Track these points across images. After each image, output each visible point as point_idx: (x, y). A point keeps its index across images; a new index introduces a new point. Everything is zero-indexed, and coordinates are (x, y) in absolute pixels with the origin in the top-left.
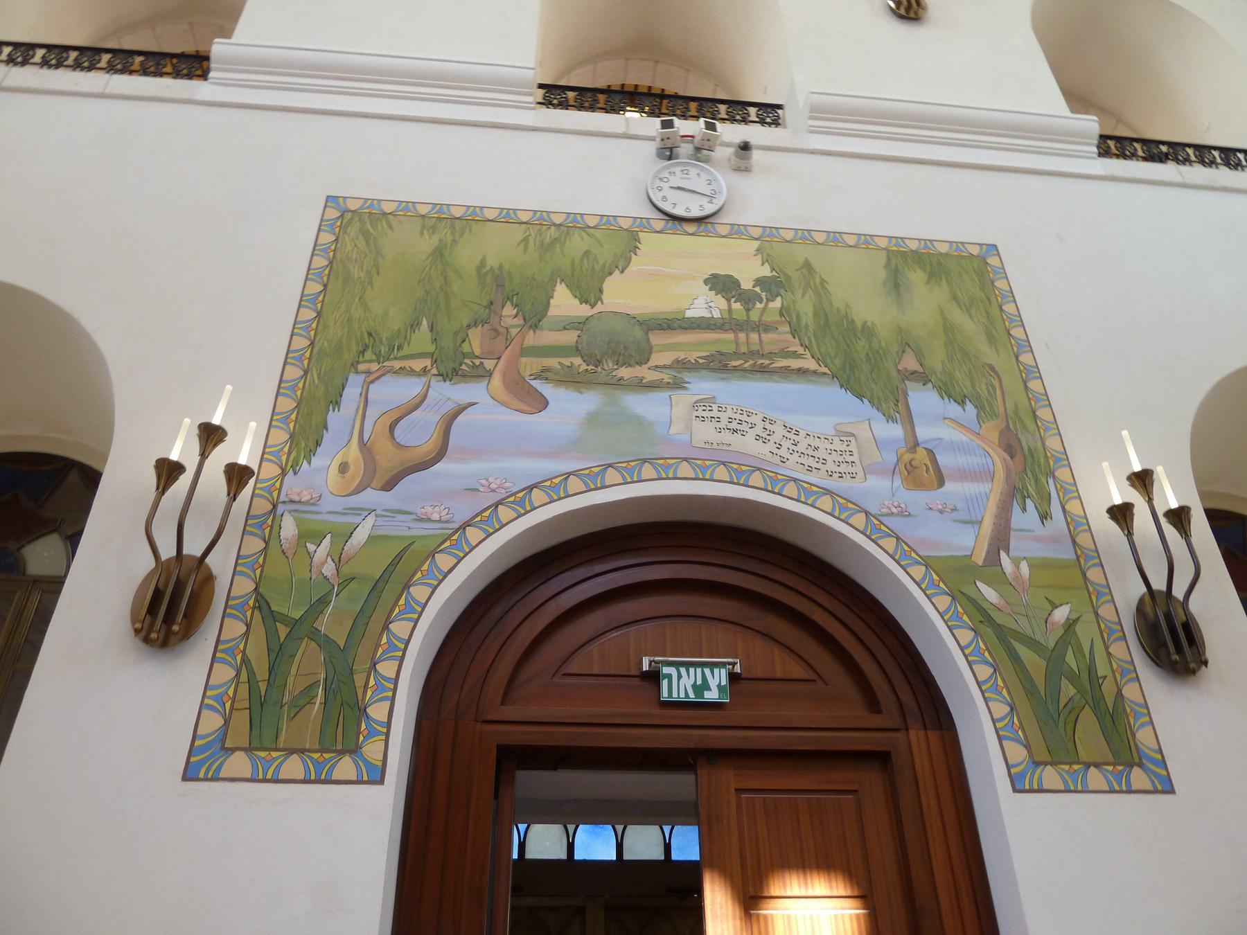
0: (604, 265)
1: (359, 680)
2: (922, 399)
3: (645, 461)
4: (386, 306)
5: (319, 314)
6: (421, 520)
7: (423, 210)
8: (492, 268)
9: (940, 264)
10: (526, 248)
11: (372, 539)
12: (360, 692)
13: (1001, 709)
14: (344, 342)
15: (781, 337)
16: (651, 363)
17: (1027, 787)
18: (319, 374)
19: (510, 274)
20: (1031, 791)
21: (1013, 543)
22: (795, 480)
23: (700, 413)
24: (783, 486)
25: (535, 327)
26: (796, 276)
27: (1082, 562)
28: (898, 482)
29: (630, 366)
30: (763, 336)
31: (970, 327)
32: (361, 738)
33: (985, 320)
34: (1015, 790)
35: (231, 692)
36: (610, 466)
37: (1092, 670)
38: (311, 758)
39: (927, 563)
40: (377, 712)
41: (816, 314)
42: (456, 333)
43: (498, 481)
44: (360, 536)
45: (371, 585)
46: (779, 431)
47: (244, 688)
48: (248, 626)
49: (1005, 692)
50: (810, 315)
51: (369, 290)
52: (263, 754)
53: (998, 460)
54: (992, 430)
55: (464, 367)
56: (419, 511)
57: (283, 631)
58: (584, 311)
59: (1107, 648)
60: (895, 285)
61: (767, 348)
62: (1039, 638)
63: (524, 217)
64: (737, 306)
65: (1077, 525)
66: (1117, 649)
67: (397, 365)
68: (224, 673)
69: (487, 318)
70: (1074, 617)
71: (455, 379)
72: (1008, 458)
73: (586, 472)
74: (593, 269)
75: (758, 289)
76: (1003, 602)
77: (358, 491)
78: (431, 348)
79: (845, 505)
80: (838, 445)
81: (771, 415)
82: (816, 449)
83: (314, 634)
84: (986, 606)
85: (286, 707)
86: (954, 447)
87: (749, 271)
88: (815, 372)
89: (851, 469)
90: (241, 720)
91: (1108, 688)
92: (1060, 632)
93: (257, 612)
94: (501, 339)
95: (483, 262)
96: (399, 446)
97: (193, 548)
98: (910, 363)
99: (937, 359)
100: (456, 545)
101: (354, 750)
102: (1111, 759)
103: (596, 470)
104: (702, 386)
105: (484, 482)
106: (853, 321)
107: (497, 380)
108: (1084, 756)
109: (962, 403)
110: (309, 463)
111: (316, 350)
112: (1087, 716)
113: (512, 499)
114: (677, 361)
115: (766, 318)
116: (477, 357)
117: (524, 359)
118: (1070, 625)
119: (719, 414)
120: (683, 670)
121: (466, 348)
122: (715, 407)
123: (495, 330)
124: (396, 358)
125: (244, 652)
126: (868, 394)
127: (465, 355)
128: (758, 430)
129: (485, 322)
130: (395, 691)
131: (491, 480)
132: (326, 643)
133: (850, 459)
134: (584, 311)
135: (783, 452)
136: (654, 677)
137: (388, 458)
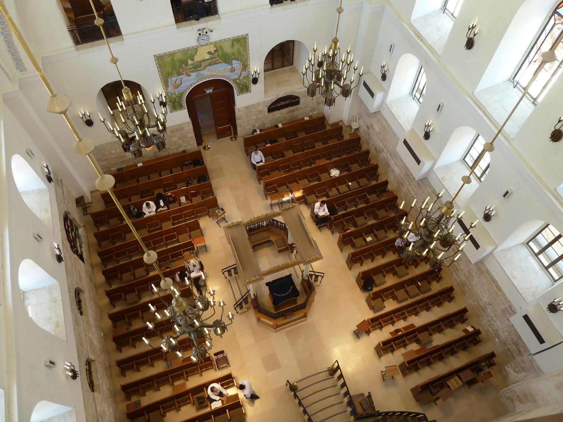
2: (234, 62)
4: (169, 69)
15: (218, 58)
31: (241, 49)
58: (193, 62)
60: (233, 45)
87: (212, 49)
98: (233, 57)
99: (236, 56)
134: (193, 62)
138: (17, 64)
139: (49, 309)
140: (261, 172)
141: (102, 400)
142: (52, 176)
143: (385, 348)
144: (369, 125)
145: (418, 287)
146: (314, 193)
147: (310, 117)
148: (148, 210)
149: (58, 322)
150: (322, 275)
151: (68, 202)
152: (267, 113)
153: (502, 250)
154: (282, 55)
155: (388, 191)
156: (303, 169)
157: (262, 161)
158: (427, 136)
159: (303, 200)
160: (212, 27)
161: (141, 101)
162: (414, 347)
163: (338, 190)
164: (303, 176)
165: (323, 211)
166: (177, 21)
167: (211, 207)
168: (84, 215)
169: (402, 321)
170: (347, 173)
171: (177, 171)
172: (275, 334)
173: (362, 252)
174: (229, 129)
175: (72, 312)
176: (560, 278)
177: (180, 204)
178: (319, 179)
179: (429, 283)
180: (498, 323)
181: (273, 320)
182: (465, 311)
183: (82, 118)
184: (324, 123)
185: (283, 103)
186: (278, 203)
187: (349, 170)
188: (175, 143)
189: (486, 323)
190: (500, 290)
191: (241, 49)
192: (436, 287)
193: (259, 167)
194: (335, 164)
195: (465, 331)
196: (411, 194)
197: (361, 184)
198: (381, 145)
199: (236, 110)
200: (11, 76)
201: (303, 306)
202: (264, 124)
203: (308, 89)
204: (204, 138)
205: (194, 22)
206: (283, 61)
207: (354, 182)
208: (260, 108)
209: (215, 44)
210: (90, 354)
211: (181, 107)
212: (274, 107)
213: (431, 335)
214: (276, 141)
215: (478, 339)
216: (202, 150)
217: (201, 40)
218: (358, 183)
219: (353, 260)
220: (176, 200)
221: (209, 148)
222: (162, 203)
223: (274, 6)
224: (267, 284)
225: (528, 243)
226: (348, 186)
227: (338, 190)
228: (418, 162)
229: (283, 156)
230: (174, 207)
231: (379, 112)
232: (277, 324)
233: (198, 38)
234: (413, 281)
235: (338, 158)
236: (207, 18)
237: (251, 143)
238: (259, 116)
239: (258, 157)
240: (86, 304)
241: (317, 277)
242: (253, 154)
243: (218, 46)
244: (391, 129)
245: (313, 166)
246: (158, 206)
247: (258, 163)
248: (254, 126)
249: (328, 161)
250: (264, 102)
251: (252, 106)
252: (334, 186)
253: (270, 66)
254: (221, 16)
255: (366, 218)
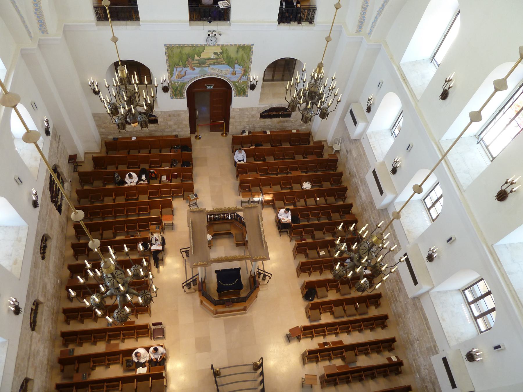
2: (237, 66)
4: (176, 60)
15: (222, 60)
31: (245, 56)
54: (243, 69)
58: (199, 58)
60: (238, 51)
79: (225, 77)
87: (219, 51)
98: (236, 62)
99: (239, 61)
104: (212, 66)
134: (199, 58)
137: (180, 76)
138: (41, 26)
139: (13, 246)
140: (240, 170)
141: (39, 340)
142: (51, 130)
143: (310, 356)
144: (348, 149)
145: (356, 308)
146: (283, 200)
147: (297, 131)
148: (130, 180)
149: (16, 259)
150: (270, 275)
151: (61, 156)
152: (259, 119)
153: (438, 292)
154: (282, 69)
155: (351, 214)
156: (279, 176)
157: (243, 160)
158: (394, 171)
159: (270, 204)
160: (221, 31)
161: (135, 80)
162: (338, 362)
163: (306, 202)
164: (276, 182)
165: (286, 217)
166: (191, 19)
167: (186, 190)
168: (74, 172)
169: (334, 336)
170: (318, 188)
171: (165, 152)
172: (214, 319)
173: (312, 263)
174: (222, 125)
175: (34, 254)
176: (485, 331)
177: (160, 181)
178: (291, 188)
179: (367, 307)
180: (422, 359)
181: (213, 306)
182: (393, 340)
183: (91, 86)
184: (309, 139)
185: (275, 113)
186: (249, 201)
187: (321, 186)
188: (170, 127)
189: (411, 356)
190: (429, 328)
191: (245, 56)
192: (373, 312)
193: (238, 165)
194: (310, 178)
195: (389, 359)
196: (371, 221)
197: (328, 202)
198: (355, 170)
199: (231, 110)
200: (33, 35)
201: (244, 300)
202: (254, 127)
203: (289, 104)
204: (198, 128)
205: (206, 23)
206: (283, 76)
207: (323, 198)
208: (253, 113)
209: (222, 46)
210: (40, 296)
211: (181, 96)
212: (266, 114)
213: (356, 355)
214: (261, 145)
215: (400, 370)
216: (193, 138)
217: (209, 40)
218: (326, 200)
219: (303, 269)
220: (157, 177)
221: (200, 138)
222: (144, 177)
223: (282, 24)
224: (216, 272)
225: (464, 291)
226: (316, 201)
227: (306, 202)
228: (382, 192)
229: (264, 160)
230: (155, 183)
231: (359, 139)
232: (216, 310)
233: (207, 38)
234: (352, 301)
235: (314, 173)
236: (219, 22)
237: (238, 142)
238: (251, 120)
239: (241, 156)
240: (50, 251)
241: (265, 276)
242: (237, 152)
243: (224, 49)
244: (366, 158)
245: (289, 175)
246: (140, 179)
247: (239, 161)
248: (245, 127)
249: (304, 174)
250: (258, 108)
251: (247, 109)
252: (303, 198)
253: (270, 77)
254: (232, 24)
255: (324, 234)
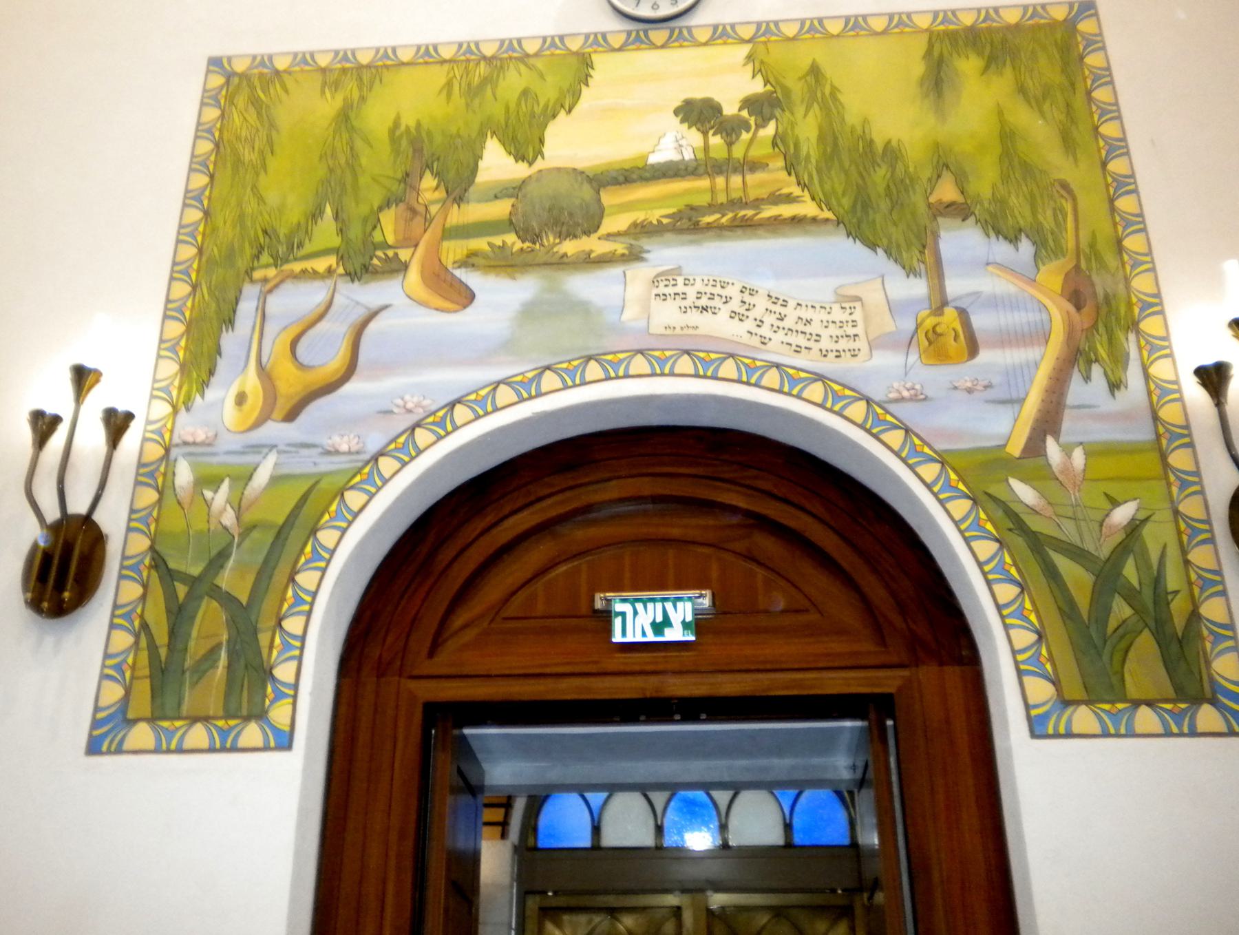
0: (546, 106)
1: (264, 639)
2: (960, 242)
3: (589, 358)
4: (284, 192)
5: (207, 213)
6: (328, 453)
7: (323, 61)
8: (408, 128)
9: (1004, 41)
10: (449, 95)
11: (276, 480)
12: (265, 652)
13: (1024, 638)
14: (236, 245)
15: (776, 176)
16: (603, 230)
17: (1051, 731)
18: (209, 288)
19: (429, 133)
20: (1057, 735)
21: (1066, 425)
22: (778, 366)
23: (662, 290)
24: (762, 376)
25: (460, 200)
26: (797, 88)
27: (1164, 442)
28: (913, 358)
29: (575, 237)
30: (749, 177)
31: (1037, 129)
32: (267, 702)
33: (1062, 117)
34: (1034, 735)
35: (130, 661)
36: (548, 368)
37: (1158, 581)
38: (215, 726)
39: (942, 460)
40: (284, 672)
41: (821, 138)
42: (365, 220)
43: (415, 399)
44: (262, 477)
45: (270, 538)
46: (761, 303)
47: (144, 656)
48: (145, 586)
49: (1033, 618)
50: (814, 140)
51: (262, 176)
52: (165, 724)
53: (1058, 315)
54: (1052, 276)
55: (375, 261)
56: (327, 442)
57: (181, 590)
58: (520, 171)
59: (1184, 552)
60: (937, 81)
61: (753, 194)
62: (1089, 546)
63: (447, 53)
64: (716, 140)
65: (1171, 390)
66: (1200, 556)
67: (297, 267)
68: (123, 640)
69: (401, 194)
70: (1142, 516)
71: (365, 276)
72: (1072, 309)
73: (519, 378)
74: (533, 115)
75: (745, 113)
76: (1043, 502)
77: (257, 424)
78: (336, 241)
79: (839, 393)
80: (838, 315)
81: (753, 283)
82: (809, 322)
83: (216, 593)
84: (1015, 507)
85: (187, 674)
86: (994, 302)
87: (732, 86)
88: (814, 220)
89: (852, 345)
90: (143, 688)
91: (1179, 607)
92: (1119, 537)
93: (154, 574)
94: (419, 220)
95: (396, 124)
96: (302, 366)
97: (78, 506)
98: (947, 192)
99: (985, 182)
100: (369, 480)
101: (260, 715)
102: (1171, 692)
103: (530, 375)
104: (665, 254)
105: (399, 402)
106: (872, 141)
107: (414, 275)
108: (1132, 691)
109: (1013, 240)
110: (203, 396)
111: (204, 259)
112: (1146, 643)
113: (431, 419)
114: (635, 225)
115: (755, 153)
116: (390, 247)
117: (445, 244)
118: (1134, 528)
119: (685, 289)
120: (639, 606)
121: (377, 236)
122: (680, 280)
123: (414, 211)
124: (296, 259)
125: (141, 616)
126: (885, 241)
127: (376, 246)
128: (735, 305)
129: (399, 201)
130: (302, 648)
131: (407, 397)
132: (227, 600)
133: (851, 331)
134: (520, 171)
135: (765, 331)
136: (605, 617)
137: (290, 382)
191: (1037, 129)
